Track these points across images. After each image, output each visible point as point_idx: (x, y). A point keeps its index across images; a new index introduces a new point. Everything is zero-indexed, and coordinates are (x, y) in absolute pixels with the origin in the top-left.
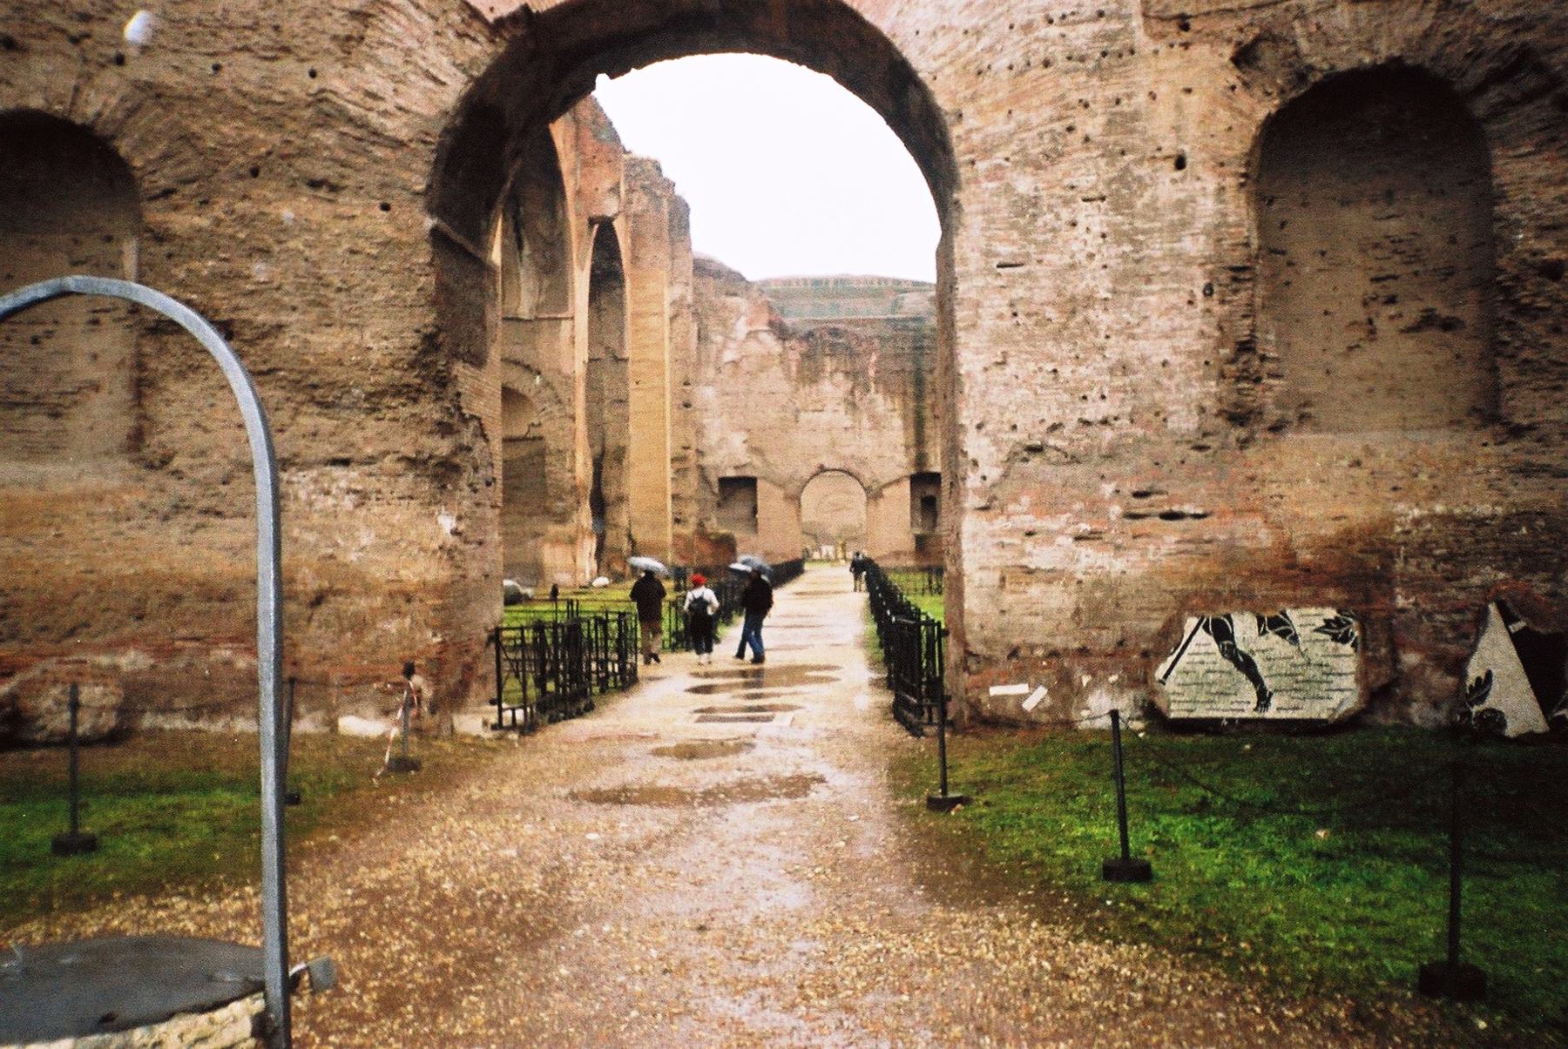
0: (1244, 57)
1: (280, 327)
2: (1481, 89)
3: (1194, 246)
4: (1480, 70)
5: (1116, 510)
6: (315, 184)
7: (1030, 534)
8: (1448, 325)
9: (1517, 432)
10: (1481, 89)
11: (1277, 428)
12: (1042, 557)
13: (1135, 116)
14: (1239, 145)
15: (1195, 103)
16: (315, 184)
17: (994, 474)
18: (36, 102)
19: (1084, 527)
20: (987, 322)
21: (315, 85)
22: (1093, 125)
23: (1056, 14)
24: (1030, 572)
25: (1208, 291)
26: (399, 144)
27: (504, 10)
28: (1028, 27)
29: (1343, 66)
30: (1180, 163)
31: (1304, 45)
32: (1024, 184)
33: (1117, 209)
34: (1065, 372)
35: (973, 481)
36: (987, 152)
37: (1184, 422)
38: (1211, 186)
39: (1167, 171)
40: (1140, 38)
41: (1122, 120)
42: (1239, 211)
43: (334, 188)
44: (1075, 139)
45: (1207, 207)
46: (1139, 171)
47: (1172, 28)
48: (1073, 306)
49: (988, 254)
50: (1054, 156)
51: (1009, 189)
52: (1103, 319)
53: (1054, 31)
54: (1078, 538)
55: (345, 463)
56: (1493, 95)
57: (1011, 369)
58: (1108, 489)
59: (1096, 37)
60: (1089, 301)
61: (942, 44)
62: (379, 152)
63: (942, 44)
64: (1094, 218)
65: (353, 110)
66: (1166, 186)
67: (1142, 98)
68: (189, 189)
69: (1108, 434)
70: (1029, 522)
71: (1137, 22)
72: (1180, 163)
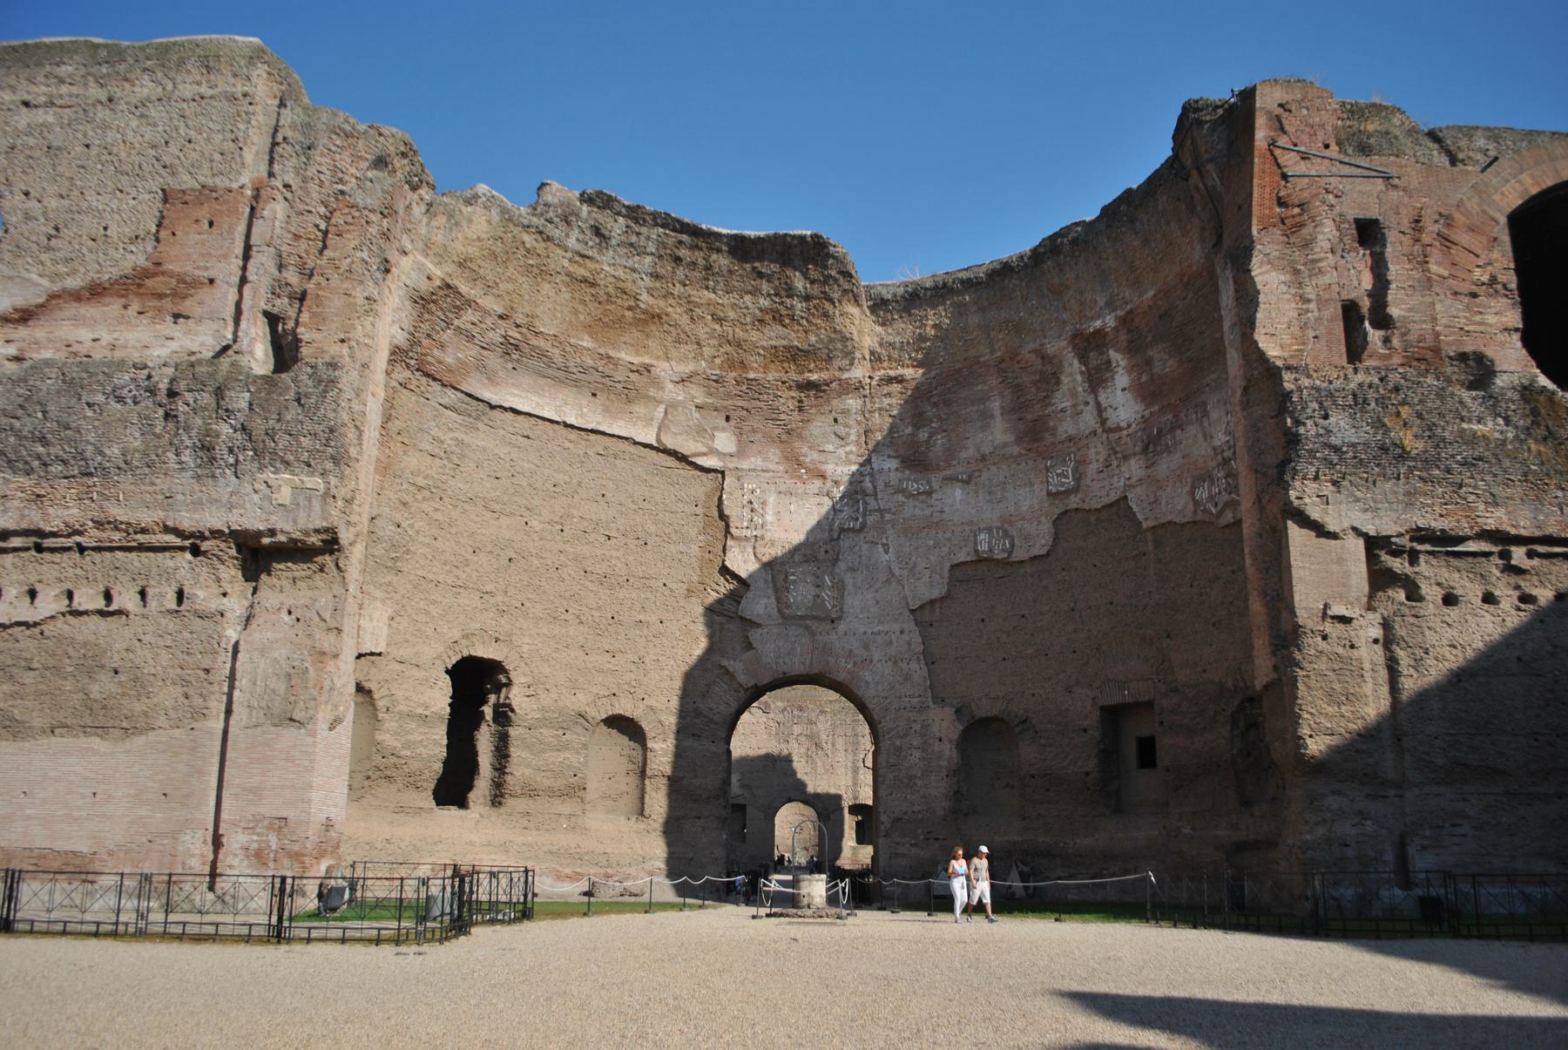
0: (958, 711)
1: (684, 777)
2: (1017, 725)
3: (943, 763)
4: (1017, 721)
5: (922, 837)
6: (694, 735)
7: (898, 844)
8: (1012, 787)
9: (1025, 818)
10: (1017, 725)
11: (966, 815)
12: (901, 850)
13: (929, 725)
14: (955, 736)
15: (945, 724)
16: (694, 735)
17: (888, 826)
18: (621, 712)
19: (913, 842)
20: (888, 782)
21: (695, 706)
22: (917, 727)
23: (908, 694)
24: (897, 854)
25: (947, 776)
26: (717, 723)
27: (750, 685)
28: (900, 698)
29: (984, 716)
30: (940, 740)
31: (974, 709)
32: (898, 743)
33: (923, 751)
34: (908, 797)
35: (882, 827)
36: (888, 733)
37: (940, 813)
38: (948, 747)
39: (937, 743)
40: (931, 704)
41: (926, 726)
42: (955, 754)
43: (699, 736)
44: (912, 731)
45: (947, 752)
46: (931, 741)
47: (940, 700)
48: (911, 778)
49: (888, 762)
50: (906, 735)
51: (894, 743)
52: (919, 782)
53: (907, 699)
54: (911, 845)
55: (699, 818)
56: (1021, 727)
57: (894, 795)
58: (920, 831)
59: (919, 702)
60: (916, 777)
61: (876, 700)
62: (712, 726)
63: (876, 700)
64: (917, 754)
65: (705, 713)
66: (936, 747)
67: (930, 721)
68: (660, 737)
69: (920, 816)
70: (898, 840)
71: (930, 698)
72: (940, 740)
